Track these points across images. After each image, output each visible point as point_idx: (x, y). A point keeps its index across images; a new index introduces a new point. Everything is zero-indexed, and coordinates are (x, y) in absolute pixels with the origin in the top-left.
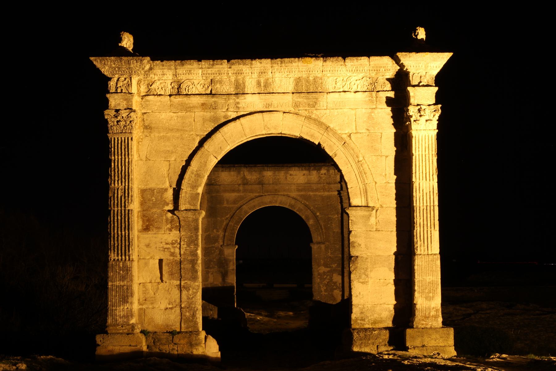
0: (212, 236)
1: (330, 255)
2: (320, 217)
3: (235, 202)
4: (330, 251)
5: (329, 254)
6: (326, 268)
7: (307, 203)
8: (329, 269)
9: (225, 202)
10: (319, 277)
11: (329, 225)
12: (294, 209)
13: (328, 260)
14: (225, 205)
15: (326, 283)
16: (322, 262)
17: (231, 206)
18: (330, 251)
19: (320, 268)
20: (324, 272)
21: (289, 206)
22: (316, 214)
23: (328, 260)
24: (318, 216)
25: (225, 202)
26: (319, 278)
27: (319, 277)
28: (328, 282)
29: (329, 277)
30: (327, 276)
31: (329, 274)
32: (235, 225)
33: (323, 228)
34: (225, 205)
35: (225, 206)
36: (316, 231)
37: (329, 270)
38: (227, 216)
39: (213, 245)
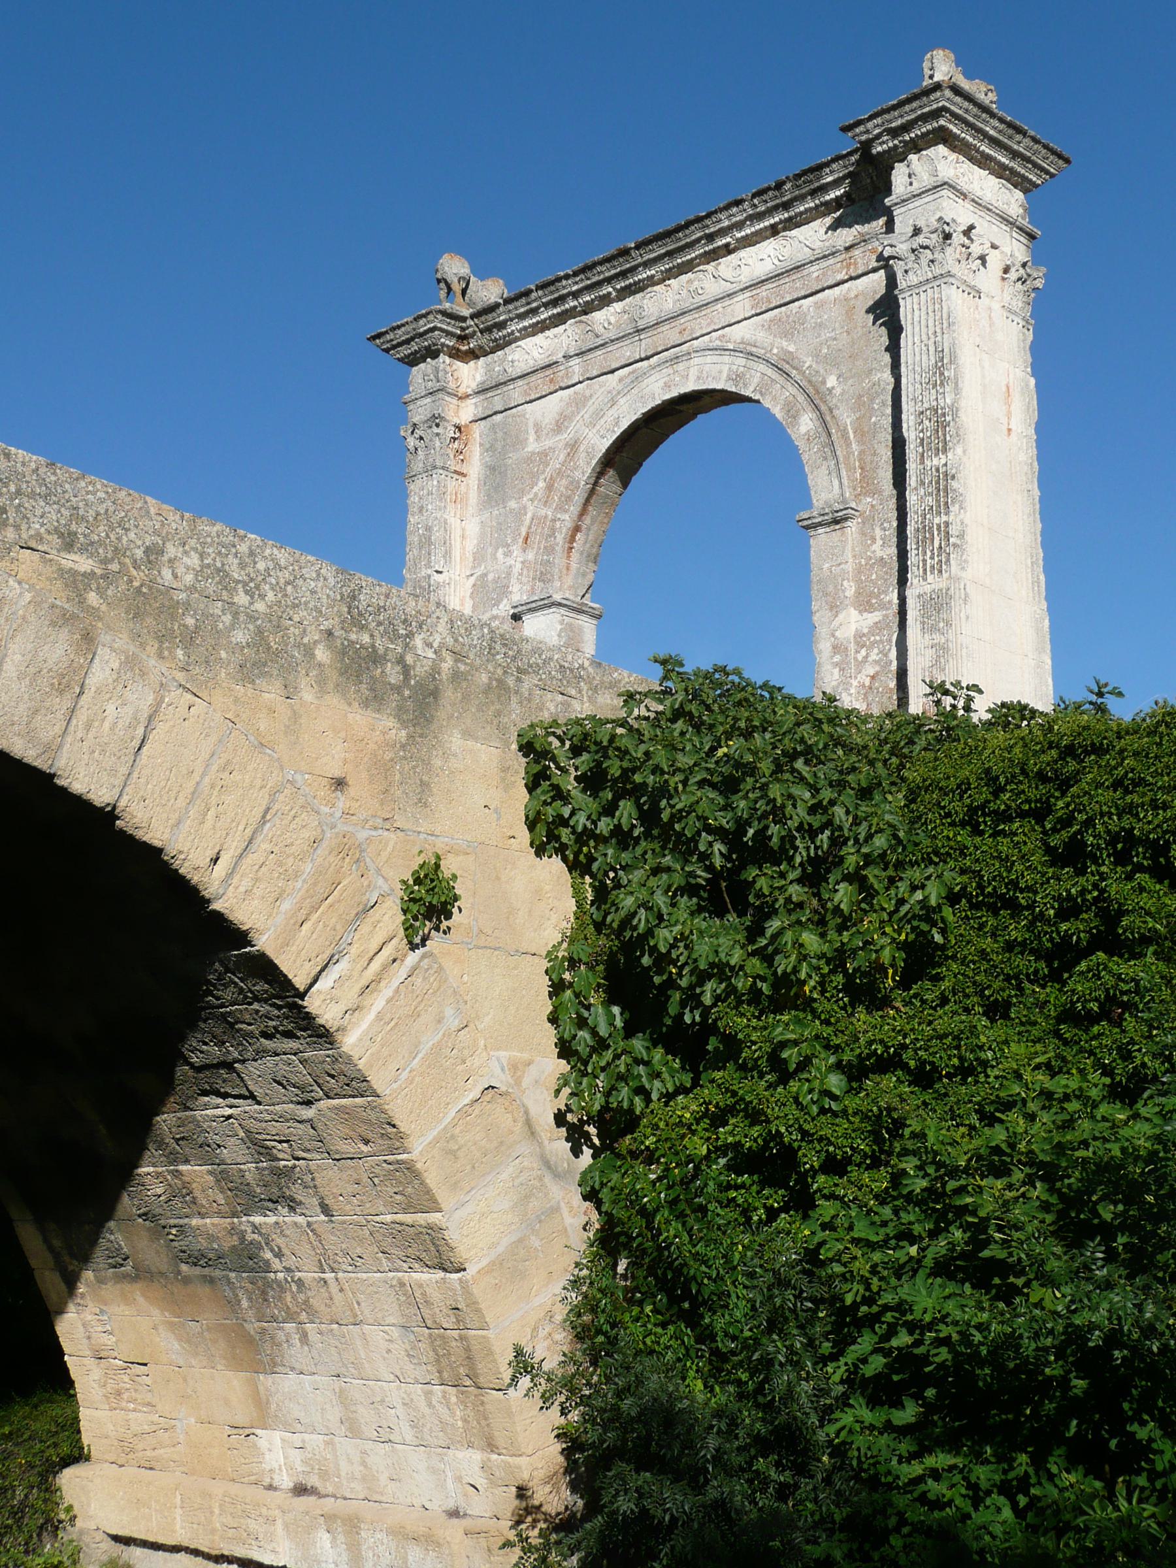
0: (490, 577)
1: (879, 554)
2: (838, 391)
3: (559, 426)
4: (878, 532)
5: (876, 547)
6: (865, 615)
7: (792, 348)
8: (876, 616)
9: (532, 437)
10: (837, 658)
11: (873, 419)
12: (745, 385)
13: (874, 577)
14: (532, 446)
15: (867, 682)
16: (850, 589)
17: (548, 443)
18: (878, 532)
19: (841, 616)
20: (859, 635)
21: (729, 379)
22: (824, 382)
23: (874, 577)
24: (830, 390)
25: (532, 437)
26: (837, 664)
27: (837, 658)
28: (873, 677)
29: (876, 651)
30: (873, 644)
31: (878, 638)
32: (559, 516)
33: (852, 436)
34: (532, 446)
35: (529, 449)
36: (825, 459)
37: (877, 620)
38: (536, 489)
39: (495, 612)
